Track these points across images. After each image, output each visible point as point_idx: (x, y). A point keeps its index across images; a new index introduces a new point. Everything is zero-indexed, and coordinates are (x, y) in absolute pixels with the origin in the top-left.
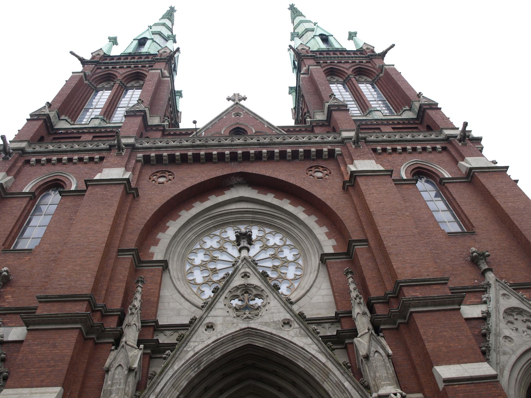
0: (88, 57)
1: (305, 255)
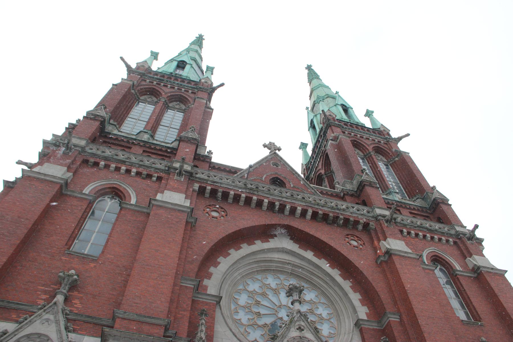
0: (134, 66)
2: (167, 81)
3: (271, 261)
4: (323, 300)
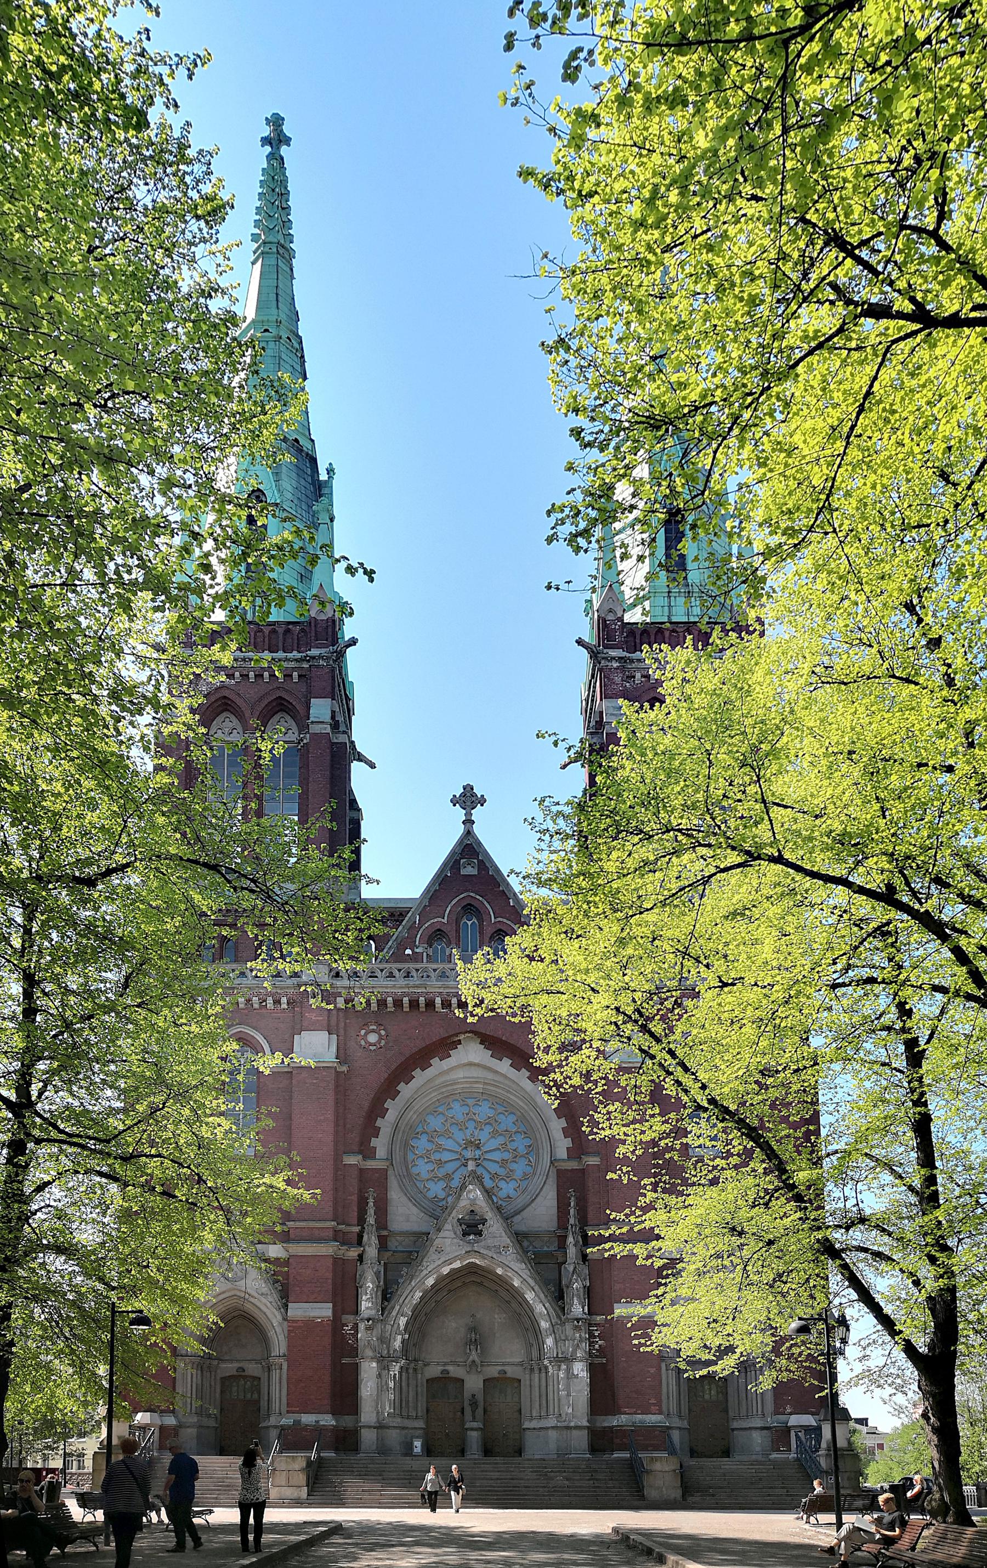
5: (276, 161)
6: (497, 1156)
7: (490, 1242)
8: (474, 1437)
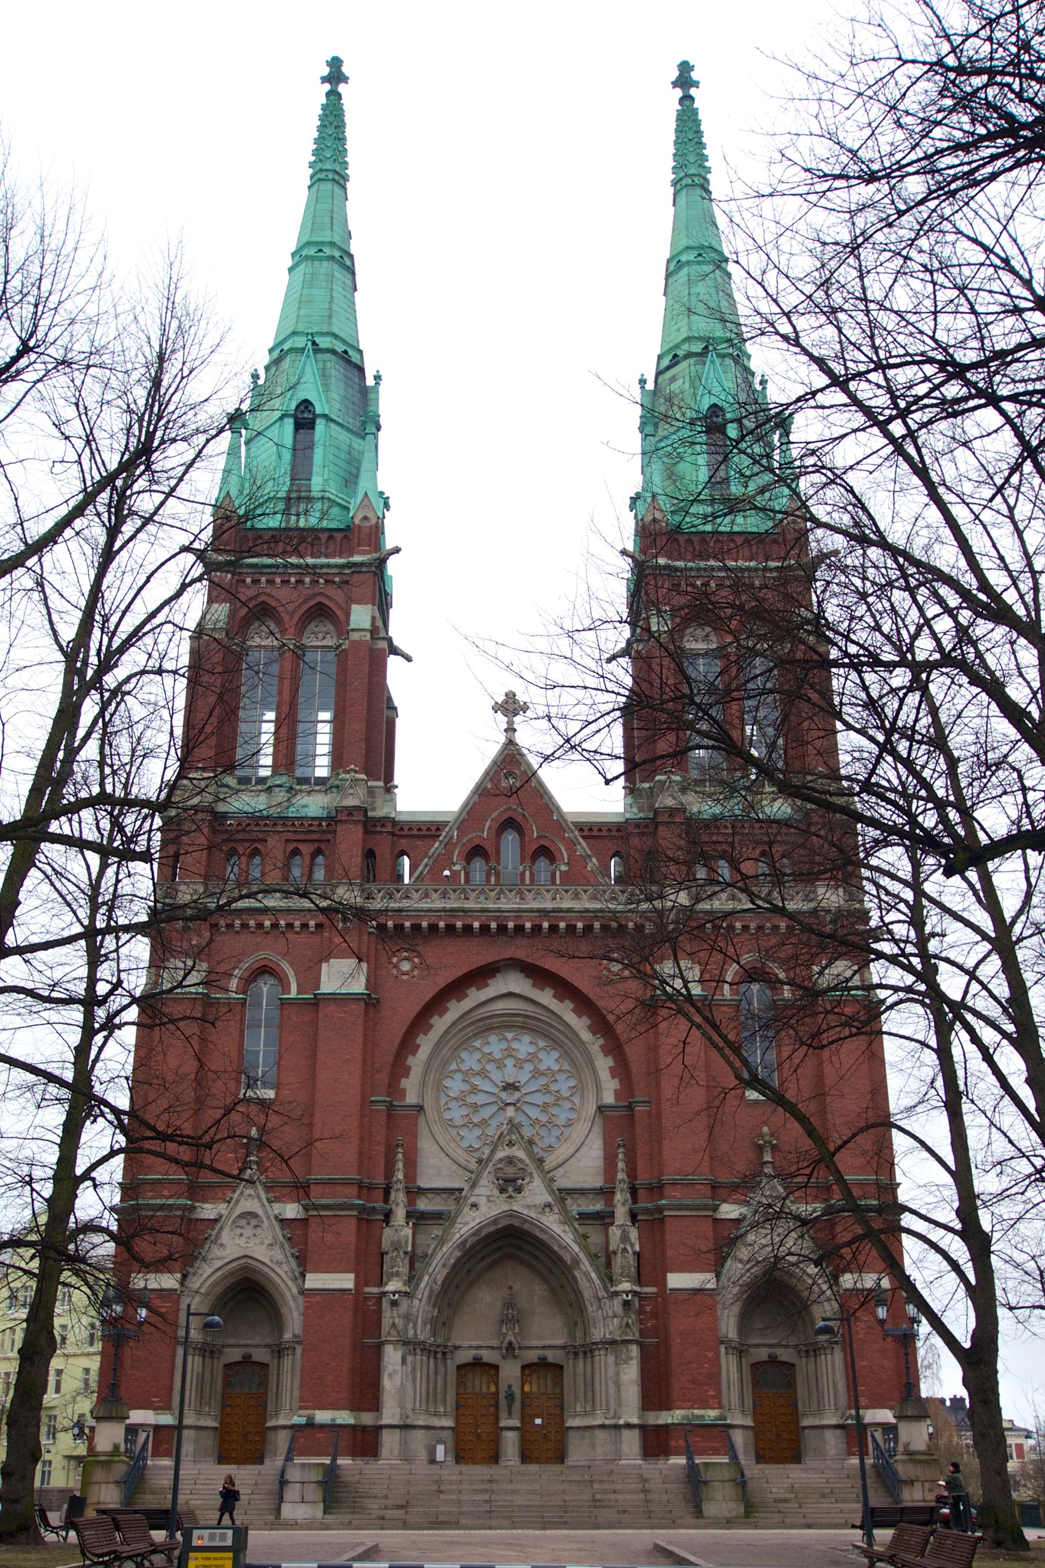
1: (582, 1090)
2: (285, 566)
3: (493, 1016)
4: (566, 1067)
5: (334, 96)
6: (539, 1099)
7: (529, 1201)
8: (510, 1441)
